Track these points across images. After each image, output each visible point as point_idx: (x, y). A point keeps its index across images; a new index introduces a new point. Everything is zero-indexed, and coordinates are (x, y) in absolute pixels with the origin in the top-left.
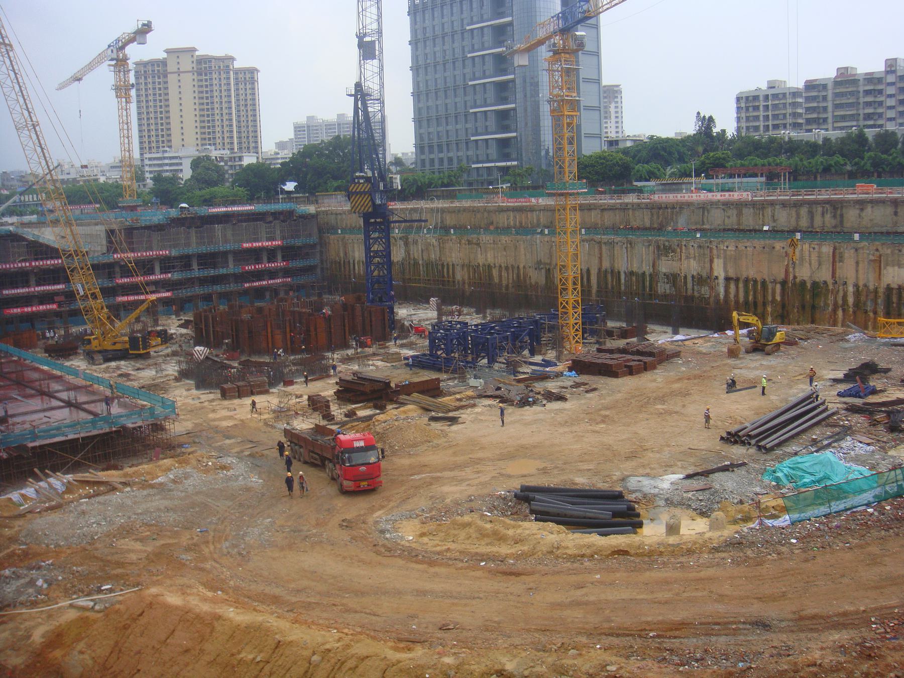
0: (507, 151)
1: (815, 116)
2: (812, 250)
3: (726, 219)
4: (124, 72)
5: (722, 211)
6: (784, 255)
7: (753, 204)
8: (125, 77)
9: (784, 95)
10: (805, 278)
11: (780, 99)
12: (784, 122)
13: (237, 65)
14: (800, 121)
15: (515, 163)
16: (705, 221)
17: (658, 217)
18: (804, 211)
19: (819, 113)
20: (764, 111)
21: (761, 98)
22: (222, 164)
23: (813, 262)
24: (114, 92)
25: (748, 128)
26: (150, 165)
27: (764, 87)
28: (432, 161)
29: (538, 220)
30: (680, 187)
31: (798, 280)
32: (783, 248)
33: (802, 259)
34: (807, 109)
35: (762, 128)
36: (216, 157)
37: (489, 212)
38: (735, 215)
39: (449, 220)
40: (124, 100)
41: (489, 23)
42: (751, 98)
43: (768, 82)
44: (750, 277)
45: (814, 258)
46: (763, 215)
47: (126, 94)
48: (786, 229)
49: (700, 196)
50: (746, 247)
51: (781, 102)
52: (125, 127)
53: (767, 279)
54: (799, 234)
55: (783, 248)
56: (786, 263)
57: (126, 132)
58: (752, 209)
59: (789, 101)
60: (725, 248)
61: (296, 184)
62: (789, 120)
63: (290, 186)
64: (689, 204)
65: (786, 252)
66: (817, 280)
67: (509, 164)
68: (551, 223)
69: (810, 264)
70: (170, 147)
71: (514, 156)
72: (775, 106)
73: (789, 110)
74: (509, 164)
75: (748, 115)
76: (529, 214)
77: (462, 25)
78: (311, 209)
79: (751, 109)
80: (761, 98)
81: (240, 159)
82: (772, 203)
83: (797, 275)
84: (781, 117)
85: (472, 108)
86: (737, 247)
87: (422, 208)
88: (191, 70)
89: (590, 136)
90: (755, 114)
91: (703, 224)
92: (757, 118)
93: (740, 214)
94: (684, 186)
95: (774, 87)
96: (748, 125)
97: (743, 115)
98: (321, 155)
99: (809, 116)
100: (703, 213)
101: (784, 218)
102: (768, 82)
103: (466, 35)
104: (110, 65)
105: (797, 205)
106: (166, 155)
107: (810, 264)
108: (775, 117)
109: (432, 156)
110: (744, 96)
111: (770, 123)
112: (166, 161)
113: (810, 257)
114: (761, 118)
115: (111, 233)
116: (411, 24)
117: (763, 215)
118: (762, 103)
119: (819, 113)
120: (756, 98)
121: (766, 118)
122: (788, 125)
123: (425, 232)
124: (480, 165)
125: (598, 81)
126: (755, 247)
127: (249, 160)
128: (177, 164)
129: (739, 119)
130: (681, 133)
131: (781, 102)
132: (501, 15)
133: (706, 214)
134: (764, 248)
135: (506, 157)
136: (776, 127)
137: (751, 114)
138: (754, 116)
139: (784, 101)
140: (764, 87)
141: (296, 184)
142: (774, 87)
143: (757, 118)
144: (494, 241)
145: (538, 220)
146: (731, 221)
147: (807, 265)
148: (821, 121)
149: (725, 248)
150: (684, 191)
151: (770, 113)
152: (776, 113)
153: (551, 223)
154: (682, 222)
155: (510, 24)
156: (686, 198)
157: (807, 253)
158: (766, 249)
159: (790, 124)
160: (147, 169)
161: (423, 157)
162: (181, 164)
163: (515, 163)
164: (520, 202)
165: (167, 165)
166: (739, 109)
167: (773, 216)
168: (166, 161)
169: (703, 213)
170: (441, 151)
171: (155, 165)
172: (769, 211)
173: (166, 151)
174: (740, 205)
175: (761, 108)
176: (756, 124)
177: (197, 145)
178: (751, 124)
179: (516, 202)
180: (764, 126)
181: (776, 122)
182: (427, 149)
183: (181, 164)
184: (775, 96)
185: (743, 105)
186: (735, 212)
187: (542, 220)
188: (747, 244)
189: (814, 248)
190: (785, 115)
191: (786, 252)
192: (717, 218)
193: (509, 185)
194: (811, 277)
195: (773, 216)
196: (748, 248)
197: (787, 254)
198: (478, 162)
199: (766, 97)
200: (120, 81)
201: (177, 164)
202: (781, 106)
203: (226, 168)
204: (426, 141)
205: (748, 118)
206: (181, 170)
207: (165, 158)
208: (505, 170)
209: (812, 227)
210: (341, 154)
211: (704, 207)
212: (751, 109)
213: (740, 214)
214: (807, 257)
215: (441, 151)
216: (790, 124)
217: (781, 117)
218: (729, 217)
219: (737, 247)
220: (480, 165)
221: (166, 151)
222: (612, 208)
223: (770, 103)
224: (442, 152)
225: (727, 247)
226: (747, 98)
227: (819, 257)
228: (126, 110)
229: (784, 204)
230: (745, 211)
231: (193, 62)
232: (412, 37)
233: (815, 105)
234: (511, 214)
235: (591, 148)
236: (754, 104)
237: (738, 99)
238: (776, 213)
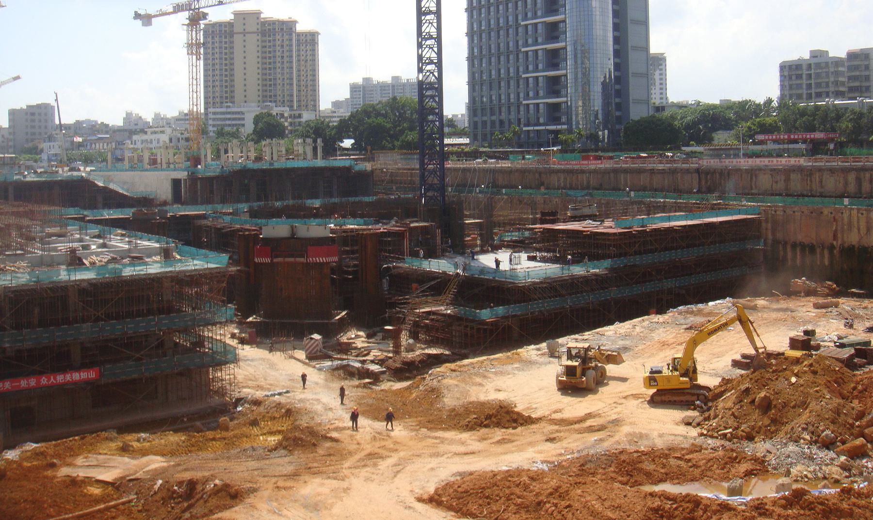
0: (557, 115)
1: (857, 84)
2: (860, 215)
3: (774, 184)
5: (770, 176)
6: (832, 219)
7: (800, 169)
9: (827, 63)
10: (854, 243)
11: (822, 68)
12: (827, 90)
13: (299, 28)
14: (842, 89)
15: (565, 127)
16: (754, 186)
17: (706, 182)
18: (852, 177)
19: (861, 82)
20: (807, 80)
21: (804, 67)
22: (282, 120)
23: (861, 227)
25: (791, 97)
26: (214, 119)
27: (807, 56)
28: (484, 123)
29: (588, 182)
30: (728, 152)
31: (846, 245)
32: (831, 213)
33: (850, 224)
34: (850, 78)
35: (805, 96)
36: (277, 114)
37: (540, 174)
38: (782, 182)
39: (500, 181)
42: (794, 67)
43: (811, 52)
44: (798, 242)
45: (863, 224)
46: (811, 181)
48: (834, 195)
49: (748, 162)
50: (794, 212)
51: (824, 70)
52: (195, 82)
53: (815, 243)
54: (847, 199)
55: (831, 213)
56: (834, 228)
57: (195, 87)
58: (799, 176)
59: (832, 70)
60: (773, 213)
61: (352, 141)
62: (832, 89)
63: (348, 143)
64: (738, 170)
65: (834, 217)
66: (866, 245)
67: (559, 127)
68: (601, 185)
69: (859, 229)
70: (233, 102)
71: (564, 119)
72: (818, 75)
73: (832, 79)
74: (559, 127)
75: (791, 83)
76: (580, 176)
78: (368, 166)
79: (794, 77)
80: (804, 67)
81: (300, 116)
82: (820, 170)
83: (845, 239)
84: (824, 85)
85: (524, 74)
86: (785, 212)
87: (475, 169)
88: (256, 30)
89: (638, 102)
90: (799, 82)
91: (752, 189)
92: (799, 86)
93: (787, 180)
94: (732, 152)
95: (817, 57)
96: (791, 92)
97: (786, 83)
98: (378, 114)
99: (852, 85)
100: (751, 178)
101: (831, 183)
102: (811, 52)
105: (845, 171)
106: (229, 110)
107: (859, 229)
108: (818, 85)
109: (485, 118)
110: (787, 64)
111: (813, 91)
112: (228, 116)
113: (858, 222)
114: (804, 86)
115: (176, 183)
117: (811, 181)
118: (805, 72)
119: (861, 82)
121: (809, 86)
122: (830, 94)
123: (478, 191)
124: (532, 128)
125: (646, 48)
126: (803, 212)
127: (307, 116)
128: (240, 119)
129: (782, 87)
130: (725, 100)
131: (824, 70)
133: (754, 178)
134: (812, 213)
135: (556, 120)
136: (819, 95)
137: (794, 82)
138: (797, 84)
139: (827, 70)
140: (807, 56)
141: (352, 141)
142: (817, 57)
143: (799, 86)
144: (545, 202)
145: (588, 182)
146: (781, 185)
147: (856, 230)
148: (864, 89)
149: (773, 213)
150: (732, 157)
151: (813, 82)
152: (819, 81)
153: (601, 185)
154: (730, 185)
156: (735, 163)
157: (856, 218)
158: (814, 214)
159: (833, 93)
160: (211, 122)
161: (476, 119)
162: (243, 119)
163: (565, 127)
164: (571, 164)
165: (229, 119)
167: (821, 182)
168: (228, 116)
169: (751, 178)
170: (492, 114)
171: (218, 119)
172: (817, 176)
173: (230, 107)
174: (788, 171)
175: (804, 77)
176: (800, 92)
177: (259, 101)
178: (794, 92)
179: (567, 164)
180: (807, 94)
181: (818, 90)
182: (479, 112)
183: (243, 119)
184: (818, 65)
185: (786, 73)
186: (783, 177)
187: (591, 182)
188: (796, 209)
189: (862, 214)
190: (827, 84)
191: (834, 217)
192: (765, 181)
193: (560, 148)
194: (859, 242)
195: (821, 182)
196: (796, 213)
197: (835, 219)
198: (528, 125)
199: (809, 66)
201: (240, 119)
202: (824, 75)
203: (286, 124)
204: (478, 104)
205: (791, 87)
206: (243, 125)
207: (229, 113)
208: (556, 132)
209: (860, 193)
210: (397, 114)
211: (753, 172)
212: (794, 77)
213: (787, 180)
214: (855, 223)
215: (492, 114)
216: (833, 93)
217: (824, 85)
218: (776, 182)
219: (785, 212)
220: (532, 128)
221: (230, 107)
222: (663, 172)
223: (813, 71)
224: (494, 115)
225: (776, 212)
226: (790, 67)
227: (867, 222)
229: (832, 171)
230: (793, 176)
231: (258, 24)
233: (858, 73)
234: (562, 176)
235: (637, 113)
236: (797, 73)
237: (783, 67)
238: (824, 180)
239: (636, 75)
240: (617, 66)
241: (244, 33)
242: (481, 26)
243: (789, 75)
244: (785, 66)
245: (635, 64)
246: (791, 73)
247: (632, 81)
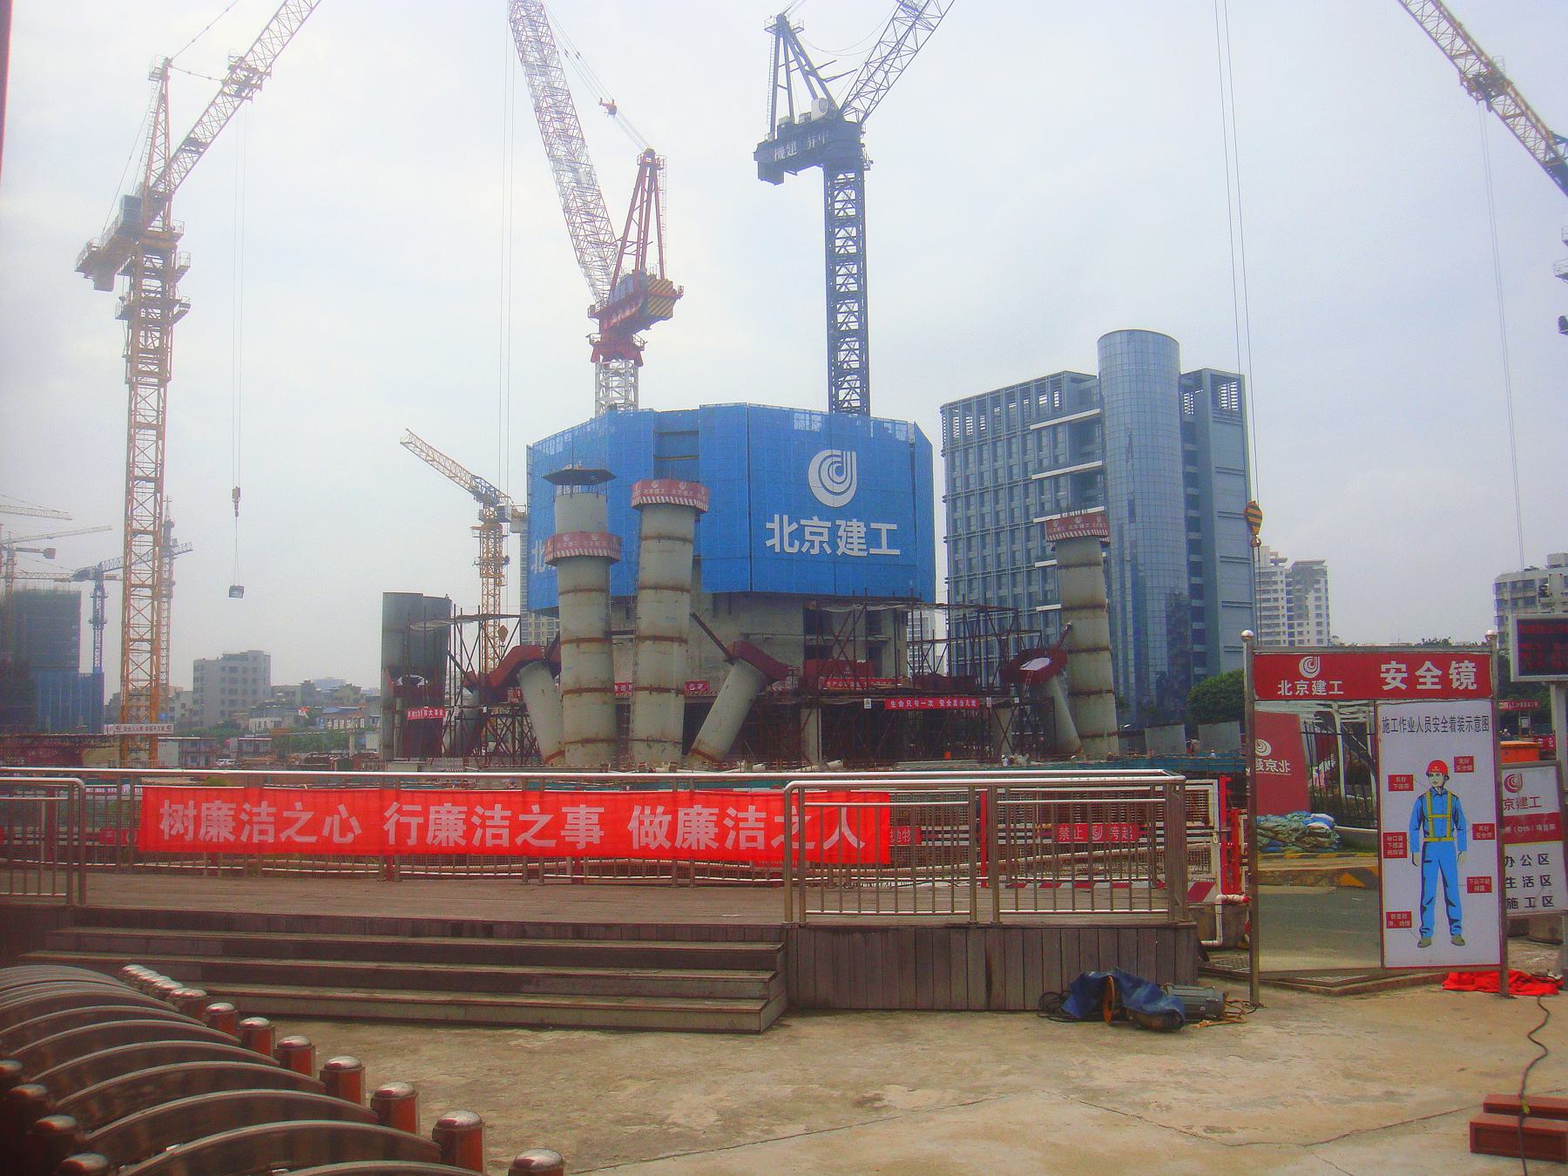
4: (495, 539)
8: (495, 547)
24: (477, 569)
40: (491, 580)
41: (1068, 470)
43: (1550, 556)
47: (495, 572)
77: (1026, 473)
79: (1520, 603)
95: (1559, 566)
102: (1550, 556)
103: (1032, 488)
104: (474, 528)
116: (947, 470)
120: (1528, 584)
125: (1248, 561)
132: (1088, 457)
142: (1559, 566)
155: (1101, 471)
166: (1500, 603)
185: (1507, 596)
200: (488, 552)
226: (1514, 584)
228: (494, 596)
232: (947, 490)
237: (1499, 587)
239: (1229, 605)
240: (1196, 591)
241: (425, 628)
242: (969, 526)
243: (1512, 599)
244: (1505, 583)
245: (1229, 584)
246: (1515, 596)
247: (1225, 619)
